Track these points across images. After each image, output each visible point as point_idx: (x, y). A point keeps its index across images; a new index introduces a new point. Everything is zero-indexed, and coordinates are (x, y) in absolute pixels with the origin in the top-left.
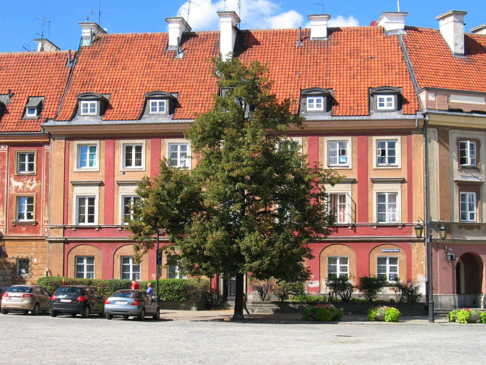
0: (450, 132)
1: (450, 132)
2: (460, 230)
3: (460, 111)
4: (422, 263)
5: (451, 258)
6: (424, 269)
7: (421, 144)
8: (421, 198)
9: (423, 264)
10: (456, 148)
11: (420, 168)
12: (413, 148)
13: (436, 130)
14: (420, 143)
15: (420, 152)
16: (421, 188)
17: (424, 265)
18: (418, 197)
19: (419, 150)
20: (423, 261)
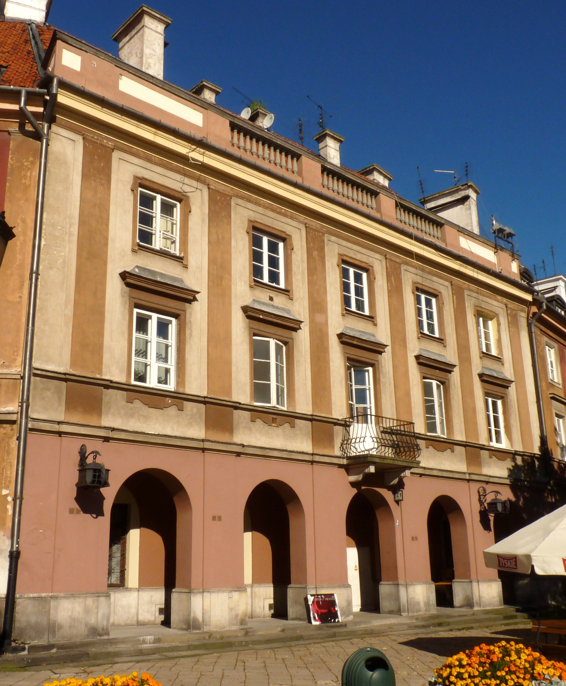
2: (130, 405)
4: (5, 492)
5: (94, 476)
6: (10, 512)
7: (33, 163)
8: (20, 303)
9: (7, 495)
11: (24, 221)
12: (9, 170)
14: (31, 159)
15: (28, 183)
16: (22, 277)
17: (10, 499)
18: (10, 298)
19: (25, 177)
20: (7, 488)
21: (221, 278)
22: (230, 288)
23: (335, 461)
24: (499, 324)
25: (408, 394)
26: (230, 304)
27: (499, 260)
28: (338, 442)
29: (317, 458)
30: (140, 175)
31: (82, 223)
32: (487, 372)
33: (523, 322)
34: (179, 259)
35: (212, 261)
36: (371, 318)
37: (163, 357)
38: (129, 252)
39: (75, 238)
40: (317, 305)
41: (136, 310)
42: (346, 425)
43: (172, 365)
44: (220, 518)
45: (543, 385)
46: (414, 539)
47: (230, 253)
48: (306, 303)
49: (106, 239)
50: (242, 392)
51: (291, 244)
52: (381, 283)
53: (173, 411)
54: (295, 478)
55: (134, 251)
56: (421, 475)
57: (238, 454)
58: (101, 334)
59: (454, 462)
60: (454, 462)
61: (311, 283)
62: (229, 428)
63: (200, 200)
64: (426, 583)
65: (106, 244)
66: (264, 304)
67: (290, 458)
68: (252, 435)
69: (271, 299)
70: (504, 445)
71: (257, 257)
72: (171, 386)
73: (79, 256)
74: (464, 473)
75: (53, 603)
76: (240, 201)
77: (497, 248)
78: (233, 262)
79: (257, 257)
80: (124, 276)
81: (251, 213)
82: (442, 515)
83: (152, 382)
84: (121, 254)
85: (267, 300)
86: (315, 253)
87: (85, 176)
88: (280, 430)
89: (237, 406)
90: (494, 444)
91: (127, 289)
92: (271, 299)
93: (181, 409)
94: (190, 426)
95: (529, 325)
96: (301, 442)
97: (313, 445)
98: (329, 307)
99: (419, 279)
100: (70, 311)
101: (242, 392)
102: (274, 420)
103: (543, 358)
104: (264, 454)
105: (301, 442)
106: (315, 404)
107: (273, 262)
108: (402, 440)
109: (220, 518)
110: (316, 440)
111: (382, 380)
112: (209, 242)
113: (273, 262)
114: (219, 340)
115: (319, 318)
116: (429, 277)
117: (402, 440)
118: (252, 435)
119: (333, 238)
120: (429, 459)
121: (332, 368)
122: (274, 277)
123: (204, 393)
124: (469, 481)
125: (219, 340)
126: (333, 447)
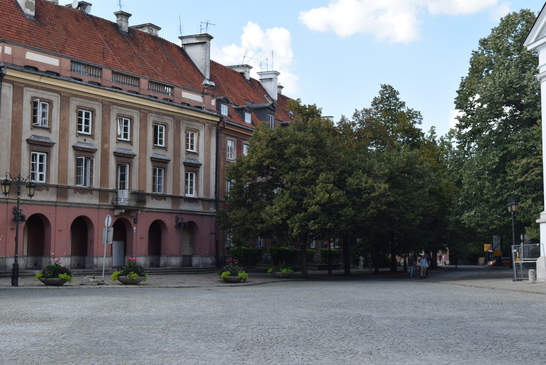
0: (25, 89)
1: (25, 89)
3: (36, 69)
10: (30, 106)
13: (11, 85)
21: (65, 134)
22: (68, 138)
23: (108, 207)
24: (199, 135)
25: (145, 176)
26: (68, 145)
27: (204, 100)
28: (110, 199)
29: (100, 207)
30: (33, 96)
31: (13, 121)
32: (188, 161)
33: (214, 132)
34: (49, 129)
35: (61, 128)
36: (130, 143)
37: (41, 169)
38: (30, 130)
39: (10, 128)
40: (105, 140)
41: (32, 152)
42: (115, 192)
43: (44, 173)
44: (61, 231)
45: (222, 163)
46: (141, 238)
47: (68, 123)
48: (100, 140)
49: (22, 126)
50: (71, 183)
51: (95, 113)
52: (137, 124)
53: (45, 191)
54: (91, 215)
55: (31, 129)
56: (147, 211)
57: (68, 206)
58: (20, 165)
59: (166, 205)
60: (166, 205)
61: (103, 131)
62: (66, 197)
63: (56, 99)
64: (145, 256)
65: (22, 128)
66: (82, 143)
67: (89, 206)
68: (75, 199)
69: (85, 140)
70: (193, 196)
71: (80, 121)
72: (44, 181)
73: (12, 135)
74: (169, 210)
75: (7, 259)
76: (74, 98)
77: (203, 94)
78: (70, 126)
79: (80, 121)
80: (28, 140)
81: (78, 102)
82: (157, 229)
83: (37, 180)
84: (27, 133)
85: (83, 141)
86: (106, 116)
87: (14, 102)
88: (86, 196)
89: (69, 187)
90: (188, 195)
91: (29, 145)
92: (85, 140)
93: (48, 190)
94: (50, 197)
95: (217, 134)
96: (94, 200)
97: (100, 201)
98: (111, 140)
99: (156, 119)
100: (9, 157)
101: (71, 183)
102: (84, 192)
103: (225, 149)
104: (79, 206)
105: (94, 200)
106: (101, 184)
107: (87, 122)
108: (140, 197)
109: (61, 231)
110: (101, 199)
111: (133, 170)
112: (60, 120)
113: (87, 122)
114: (63, 161)
115: (106, 146)
116: (162, 117)
117: (140, 197)
118: (75, 199)
119: (115, 107)
120: (151, 204)
121: (110, 167)
122: (87, 130)
123: (57, 184)
124: (171, 213)
125: (63, 161)
126: (108, 201)
